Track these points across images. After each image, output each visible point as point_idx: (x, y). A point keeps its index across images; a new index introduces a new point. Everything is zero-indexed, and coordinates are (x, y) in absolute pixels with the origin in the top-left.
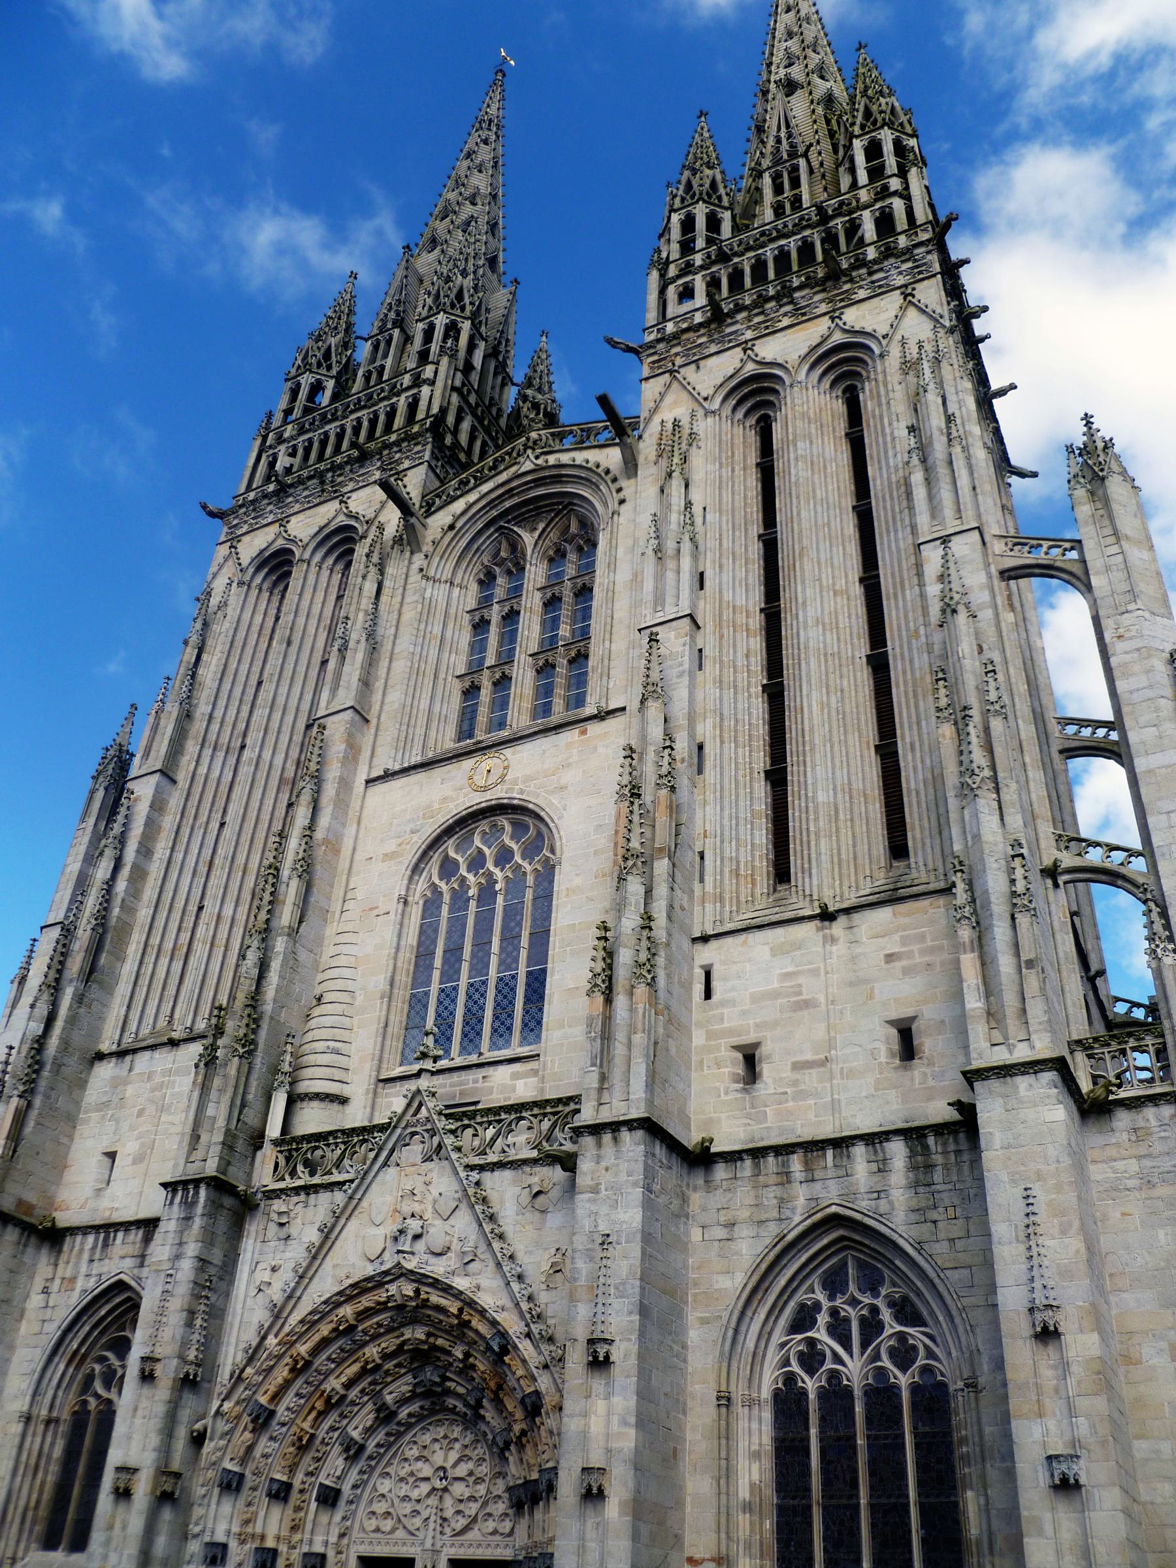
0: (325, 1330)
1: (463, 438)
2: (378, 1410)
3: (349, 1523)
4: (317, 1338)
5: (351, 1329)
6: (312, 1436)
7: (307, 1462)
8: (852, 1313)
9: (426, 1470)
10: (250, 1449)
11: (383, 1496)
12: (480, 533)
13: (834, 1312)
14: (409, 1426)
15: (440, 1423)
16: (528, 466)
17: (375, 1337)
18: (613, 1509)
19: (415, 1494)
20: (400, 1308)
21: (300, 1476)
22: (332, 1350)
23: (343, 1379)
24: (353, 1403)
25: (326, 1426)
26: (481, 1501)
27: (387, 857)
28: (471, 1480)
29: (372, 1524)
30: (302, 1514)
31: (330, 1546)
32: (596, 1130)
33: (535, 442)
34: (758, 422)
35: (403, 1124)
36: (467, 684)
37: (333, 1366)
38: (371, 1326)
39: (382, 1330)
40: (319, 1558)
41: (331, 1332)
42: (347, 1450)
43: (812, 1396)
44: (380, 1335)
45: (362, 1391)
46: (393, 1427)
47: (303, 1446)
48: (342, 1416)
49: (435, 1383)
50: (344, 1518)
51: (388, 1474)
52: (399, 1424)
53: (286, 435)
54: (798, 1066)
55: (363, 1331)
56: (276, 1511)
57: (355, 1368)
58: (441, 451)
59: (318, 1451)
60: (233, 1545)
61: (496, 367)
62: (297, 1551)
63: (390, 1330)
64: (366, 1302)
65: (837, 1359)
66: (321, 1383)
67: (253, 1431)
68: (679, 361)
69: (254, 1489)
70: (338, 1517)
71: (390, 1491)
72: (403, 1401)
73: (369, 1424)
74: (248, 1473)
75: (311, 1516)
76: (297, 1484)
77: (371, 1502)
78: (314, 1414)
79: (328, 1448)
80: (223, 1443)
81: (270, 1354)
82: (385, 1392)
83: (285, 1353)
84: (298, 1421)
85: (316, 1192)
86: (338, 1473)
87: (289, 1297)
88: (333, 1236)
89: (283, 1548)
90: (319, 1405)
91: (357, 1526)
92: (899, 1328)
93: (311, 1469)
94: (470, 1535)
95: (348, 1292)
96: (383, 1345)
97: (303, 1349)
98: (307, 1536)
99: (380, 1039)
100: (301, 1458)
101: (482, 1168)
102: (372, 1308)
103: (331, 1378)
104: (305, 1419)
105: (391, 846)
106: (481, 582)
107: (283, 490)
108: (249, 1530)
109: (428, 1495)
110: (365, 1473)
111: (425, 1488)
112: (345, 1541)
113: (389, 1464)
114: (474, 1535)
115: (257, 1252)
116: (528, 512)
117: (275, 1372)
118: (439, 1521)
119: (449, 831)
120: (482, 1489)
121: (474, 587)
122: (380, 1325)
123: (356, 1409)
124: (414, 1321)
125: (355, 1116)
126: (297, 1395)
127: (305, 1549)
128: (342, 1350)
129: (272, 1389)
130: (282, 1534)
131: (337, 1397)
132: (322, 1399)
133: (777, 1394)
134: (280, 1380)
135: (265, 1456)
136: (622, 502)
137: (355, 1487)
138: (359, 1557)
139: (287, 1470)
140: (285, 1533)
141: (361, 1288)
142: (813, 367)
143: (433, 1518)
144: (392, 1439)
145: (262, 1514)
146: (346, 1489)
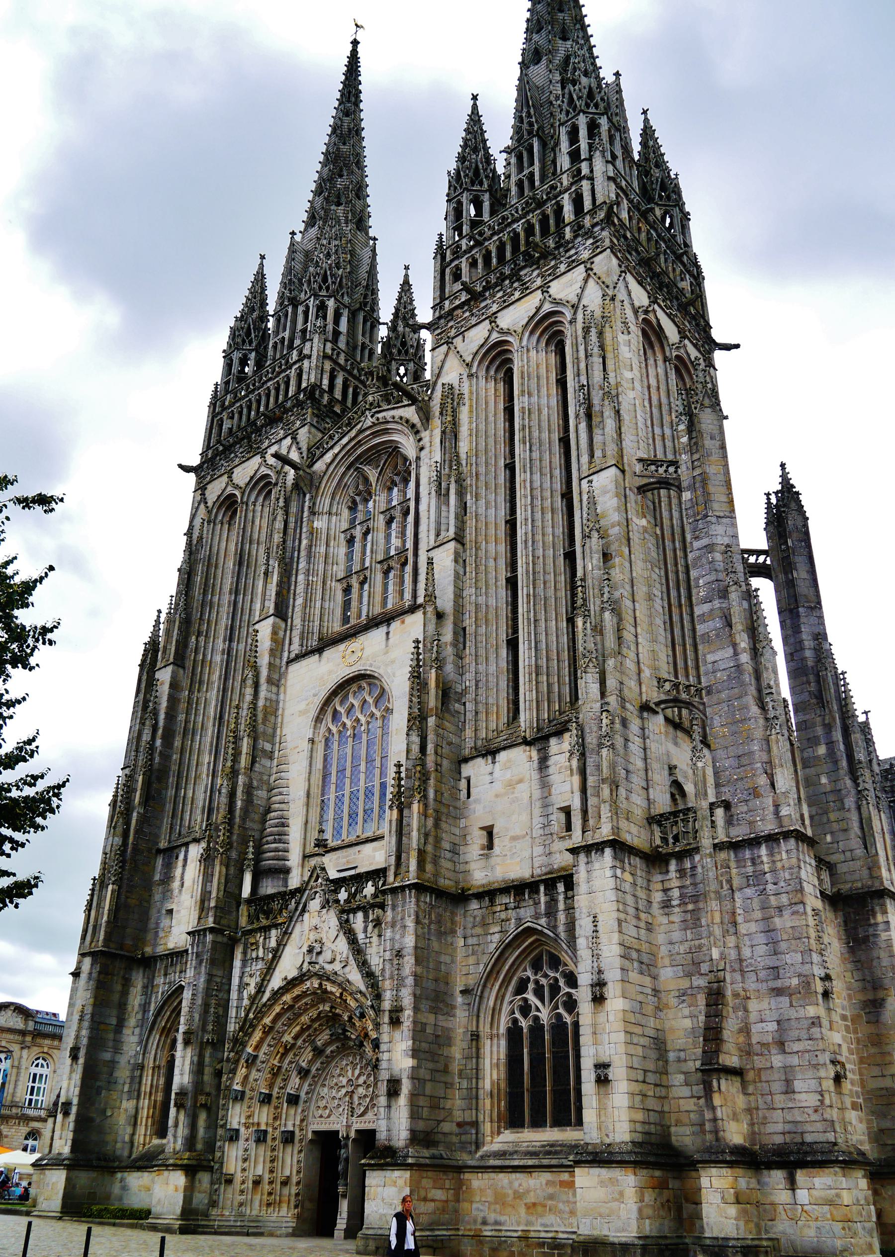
0: (277, 1009)
1: (338, 394)
2: (313, 1050)
4: (274, 1014)
5: (291, 1007)
6: (280, 1068)
7: (279, 1082)
8: (544, 981)
12: (344, 474)
13: (537, 982)
14: (333, 1058)
15: (348, 1055)
16: (369, 423)
17: (306, 1010)
18: (403, 1100)
20: (314, 993)
21: (276, 1090)
22: (283, 1019)
25: (287, 1061)
27: (303, 713)
32: (394, 891)
33: (371, 404)
34: (505, 374)
36: (345, 585)
42: (299, 1073)
43: (525, 1031)
46: (323, 1059)
47: (276, 1073)
52: (327, 1057)
53: (227, 403)
54: (514, 838)
56: (265, 1109)
57: (298, 1028)
58: (319, 410)
60: (242, 1130)
61: (364, 317)
63: (312, 1006)
64: (297, 991)
65: (538, 1010)
68: (453, 332)
69: (251, 1098)
70: (300, 1110)
72: (327, 1044)
74: (247, 1091)
75: (284, 1111)
76: (275, 1094)
89: (270, 1130)
90: (281, 1050)
92: (568, 990)
94: (366, 1117)
97: (267, 1020)
101: (348, 912)
105: (302, 706)
106: (350, 508)
107: (228, 449)
111: (344, 1091)
113: (325, 1079)
116: (371, 456)
119: (334, 693)
121: (346, 513)
122: (306, 1004)
124: (323, 1001)
125: (294, 882)
127: (283, 1129)
129: (254, 1043)
133: (509, 1030)
135: (256, 1080)
136: (422, 449)
137: (307, 1093)
140: (271, 1121)
141: (290, 984)
142: (532, 333)
146: (303, 1095)
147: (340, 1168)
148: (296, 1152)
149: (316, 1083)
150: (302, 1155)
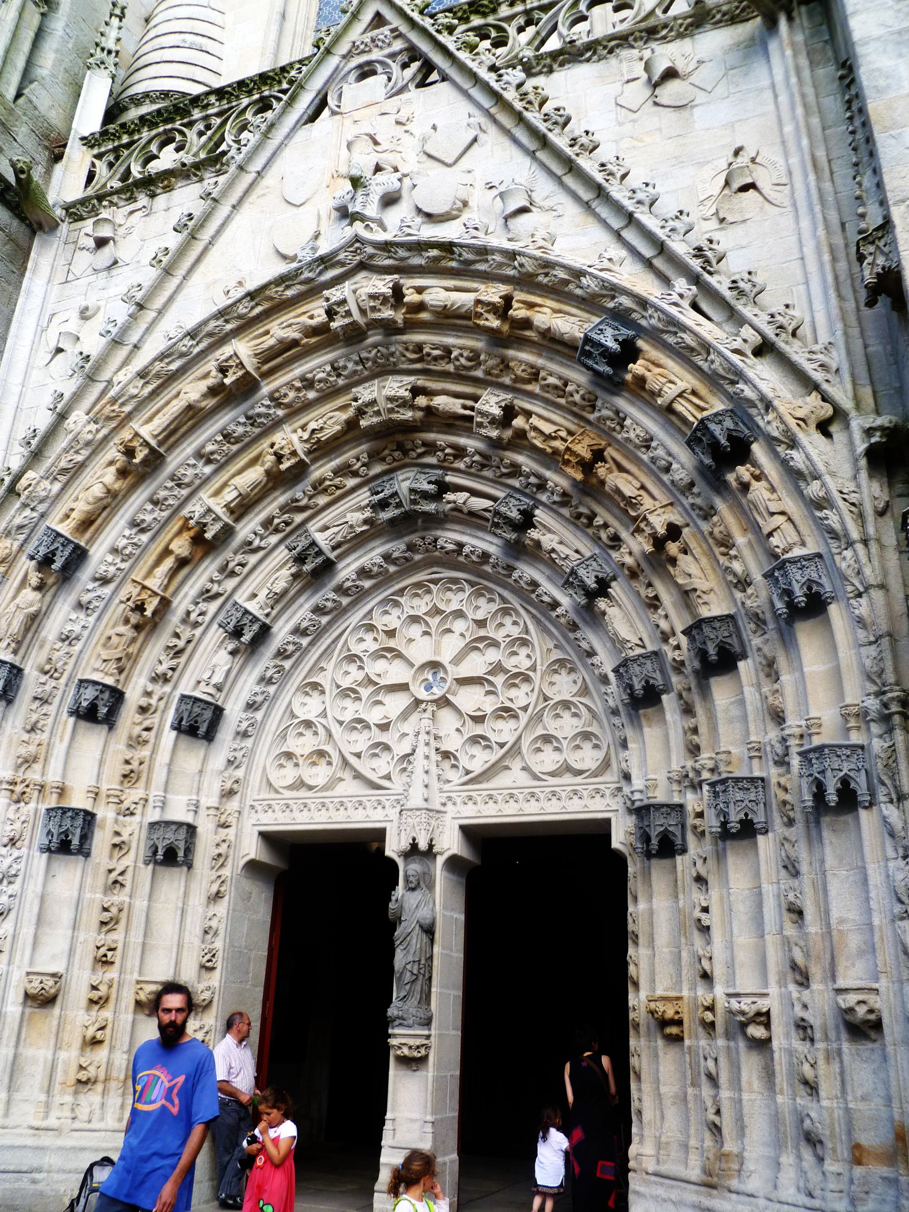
2: (300, 559)
3: (240, 773)
4: (176, 407)
6: (165, 604)
9: (395, 672)
10: (34, 621)
11: (308, 724)
19: (375, 716)
23: (229, 495)
24: (248, 547)
26: (524, 718)
28: (499, 680)
30: (145, 752)
31: (202, 812)
35: (344, 47)
37: (208, 470)
38: (290, 385)
39: (311, 395)
40: (182, 834)
41: (205, 396)
44: (308, 406)
45: (267, 523)
46: (326, 595)
48: (227, 572)
49: (425, 495)
50: (230, 762)
51: (315, 686)
52: (340, 590)
55: (272, 398)
59: (177, 636)
62: (137, 818)
63: (330, 394)
67: (39, 588)
71: (324, 714)
73: (279, 586)
75: (163, 756)
76: (133, 696)
77: (283, 736)
78: (169, 563)
79: (198, 632)
81: (75, 439)
82: (313, 526)
83: (106, 439)
84: (138, 575)
85: (168, 189)
86: (218, 678)
87: (117, 342)
88: (205, 235)
91: (255, 779)
93: (161, 669)
94: (503, 780)
95: (242, 310)
96: (313, 425)
98: (156, 792)
99: (275, 28)
100: (140, 650)
102: (295, 343)
103: (204, 495)
104: (149, 573)
108: (34, 775)
109: (405, 715)
110: (270, 681)
112: (233, 804)
113: (317, 668)
114: (514, 777)
115: (52, 298)
118: (435, 757)
120: (520, 696)
123: (253, 559)
126: (134, 524)
127: (154, 816)
128: (227, 436)
129: (81, 508)
130: (104, 787)
131: (218, 526)
132: (186, 536)
134: (98, 491)
135: (66, 639)
137: (251, 706)
138: (261, 834)
139: (112, 667)
143: (421, 750)
144: (325, 620)
145: (60, 749)
146: (234, 711)
147: (400, 959)
148: (197, 900)
149: (284, 675)
150: (221, 908)
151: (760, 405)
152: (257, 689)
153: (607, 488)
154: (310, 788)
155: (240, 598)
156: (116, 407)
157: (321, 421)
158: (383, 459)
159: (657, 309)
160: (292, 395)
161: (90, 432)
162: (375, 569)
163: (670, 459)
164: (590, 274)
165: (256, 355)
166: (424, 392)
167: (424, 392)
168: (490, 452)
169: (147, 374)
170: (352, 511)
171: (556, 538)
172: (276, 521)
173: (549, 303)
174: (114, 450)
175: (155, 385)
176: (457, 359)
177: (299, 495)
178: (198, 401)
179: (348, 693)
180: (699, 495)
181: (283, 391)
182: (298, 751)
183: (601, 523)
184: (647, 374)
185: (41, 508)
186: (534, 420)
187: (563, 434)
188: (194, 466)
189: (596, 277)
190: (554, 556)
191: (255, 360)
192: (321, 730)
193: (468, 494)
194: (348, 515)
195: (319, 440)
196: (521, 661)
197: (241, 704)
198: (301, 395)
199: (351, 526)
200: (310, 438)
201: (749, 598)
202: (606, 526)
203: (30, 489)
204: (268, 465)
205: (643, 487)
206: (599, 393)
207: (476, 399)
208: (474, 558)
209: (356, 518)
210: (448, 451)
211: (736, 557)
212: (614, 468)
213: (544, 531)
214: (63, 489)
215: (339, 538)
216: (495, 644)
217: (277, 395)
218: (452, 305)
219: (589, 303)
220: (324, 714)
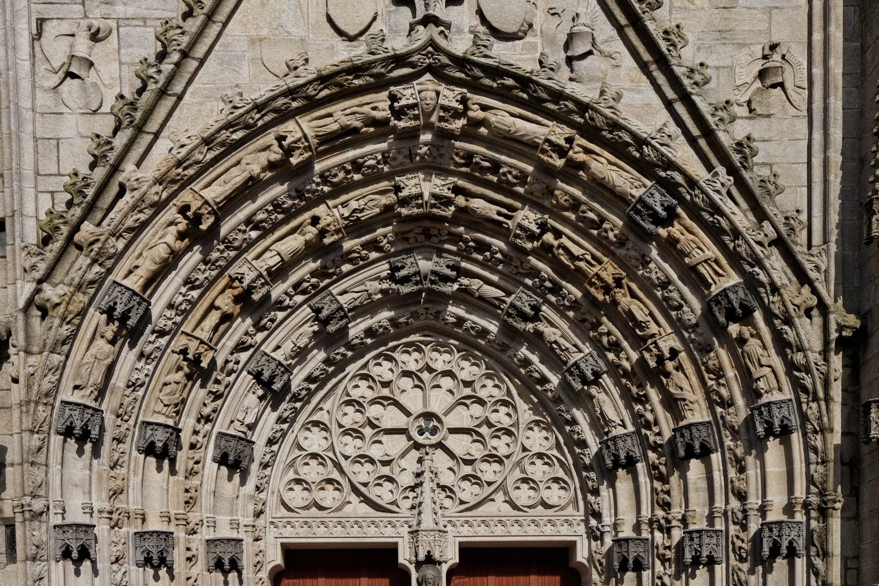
4: (236, 177)
9: (391, 418)
14: (359, 351)
24: (279, 305)
29: (298, 497)
37: (254, 234)
38: (341, 166)
39: (357, 177)
41: (264, 170)
55: (322, 175)
57: (295, 243)
66: (231, 262)
73: (302, 343)
80: (56, 359)
81: (142, 199)
96: (354, 205)
102: (355, 130)
112: (261, 522)
117: (147, 235)
120: (501, 446)
122: (357, 166)
126: (187, 282)
137: (271, 442)
151: (768, 288)
152: (278, 427)
153: (619, 308)
154: (321, 508)
155: (267, 348)
156: (180, 170)
157: (362, 202)
158: (407, 239)
159: (703, 192)
160: (341, 175)
161: (157, 193)
162: (381, 330)
163: (683, 302)
164: (653, 147)
165: (317, 136)
166: (468, 194)
167: (468, 194)
168: (513, 254)
169: (212, 141)
170: (371, 280)
171: (559, 333)
172: (306, 285)
173: (606, 154)
174: (174, 210)
175: (217, 152)
176: (504, 174)
177: (329, 264)
178: (259, 175)
179: (354, 432)
180: (701, 334)
181: (334, 172)
182: (309, 479)
183: (606, 331)
184: (682, 237)
185: (109, 263)
186: (564, 240)
187: (589, 257)
188: (244, 232)
189: (657, 150)
190: (555, 346)
191: (316, 141)
192: (329, 462)
193: (481, 283)
194: (368, 283)
195: (358, 218)
196: (501, 417)
197: (264, 441)
198: (349, 176)
199: (370, 295)
200: (350, 216)
201: (729, 414)
202: (609, 334)
203: (99, 245)
204: (309, 236)
205: (651, 314)
206: (631, 237)
207: (513, 209)
208: (473, 332)
209: (375, 286)
210: (471, 244)
211: (723, 385)
212: (628, 294)
213: (547, 324)
214: (127, 247)
215: (357, 303)
216: (481, 402)
217: (327, 174)
218: (516, 132)
219: (644, 167)
220: (332, 448)
